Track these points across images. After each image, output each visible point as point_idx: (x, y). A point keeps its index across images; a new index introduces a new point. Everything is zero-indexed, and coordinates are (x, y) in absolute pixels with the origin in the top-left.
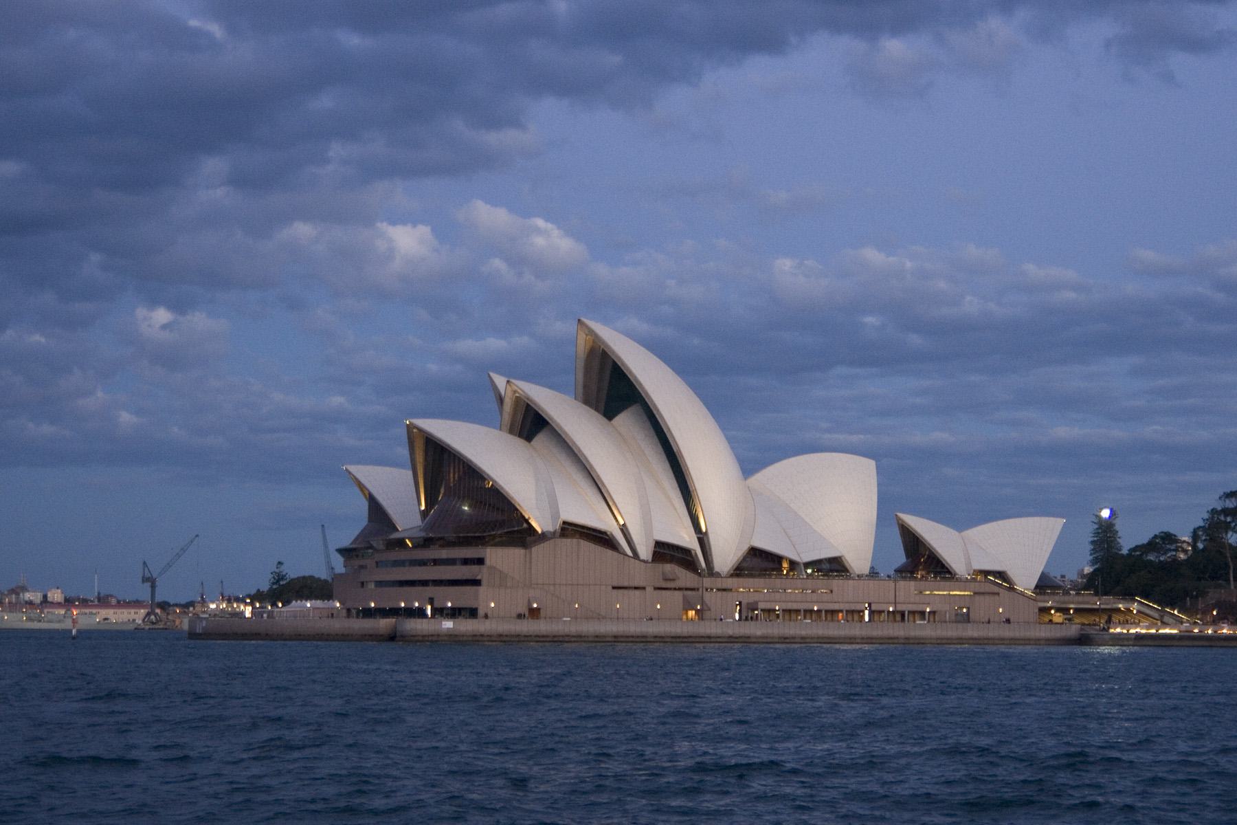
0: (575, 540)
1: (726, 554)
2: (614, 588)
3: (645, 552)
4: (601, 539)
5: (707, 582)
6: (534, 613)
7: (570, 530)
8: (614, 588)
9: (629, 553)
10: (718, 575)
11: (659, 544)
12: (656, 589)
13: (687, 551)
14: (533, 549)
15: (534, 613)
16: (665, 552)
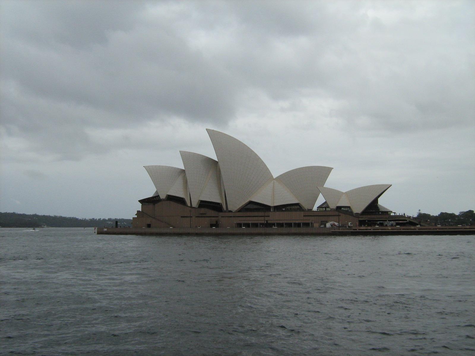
0: (169, 201)
1: (235, 204)
2: (182, 217)
3: (195, 204)
4: (180, 201)
5: (221, 214)
6: (149, 226)
7: (170, 198)
8: (182, 217)
9: (189, 205)
10: (230, 211)
11: (202, 201)
12: (196, 217)
13: (218, 204)
14: (156, 205)
15: (149, 226)
16: (203, 204)
